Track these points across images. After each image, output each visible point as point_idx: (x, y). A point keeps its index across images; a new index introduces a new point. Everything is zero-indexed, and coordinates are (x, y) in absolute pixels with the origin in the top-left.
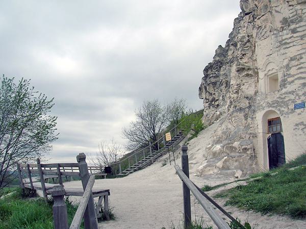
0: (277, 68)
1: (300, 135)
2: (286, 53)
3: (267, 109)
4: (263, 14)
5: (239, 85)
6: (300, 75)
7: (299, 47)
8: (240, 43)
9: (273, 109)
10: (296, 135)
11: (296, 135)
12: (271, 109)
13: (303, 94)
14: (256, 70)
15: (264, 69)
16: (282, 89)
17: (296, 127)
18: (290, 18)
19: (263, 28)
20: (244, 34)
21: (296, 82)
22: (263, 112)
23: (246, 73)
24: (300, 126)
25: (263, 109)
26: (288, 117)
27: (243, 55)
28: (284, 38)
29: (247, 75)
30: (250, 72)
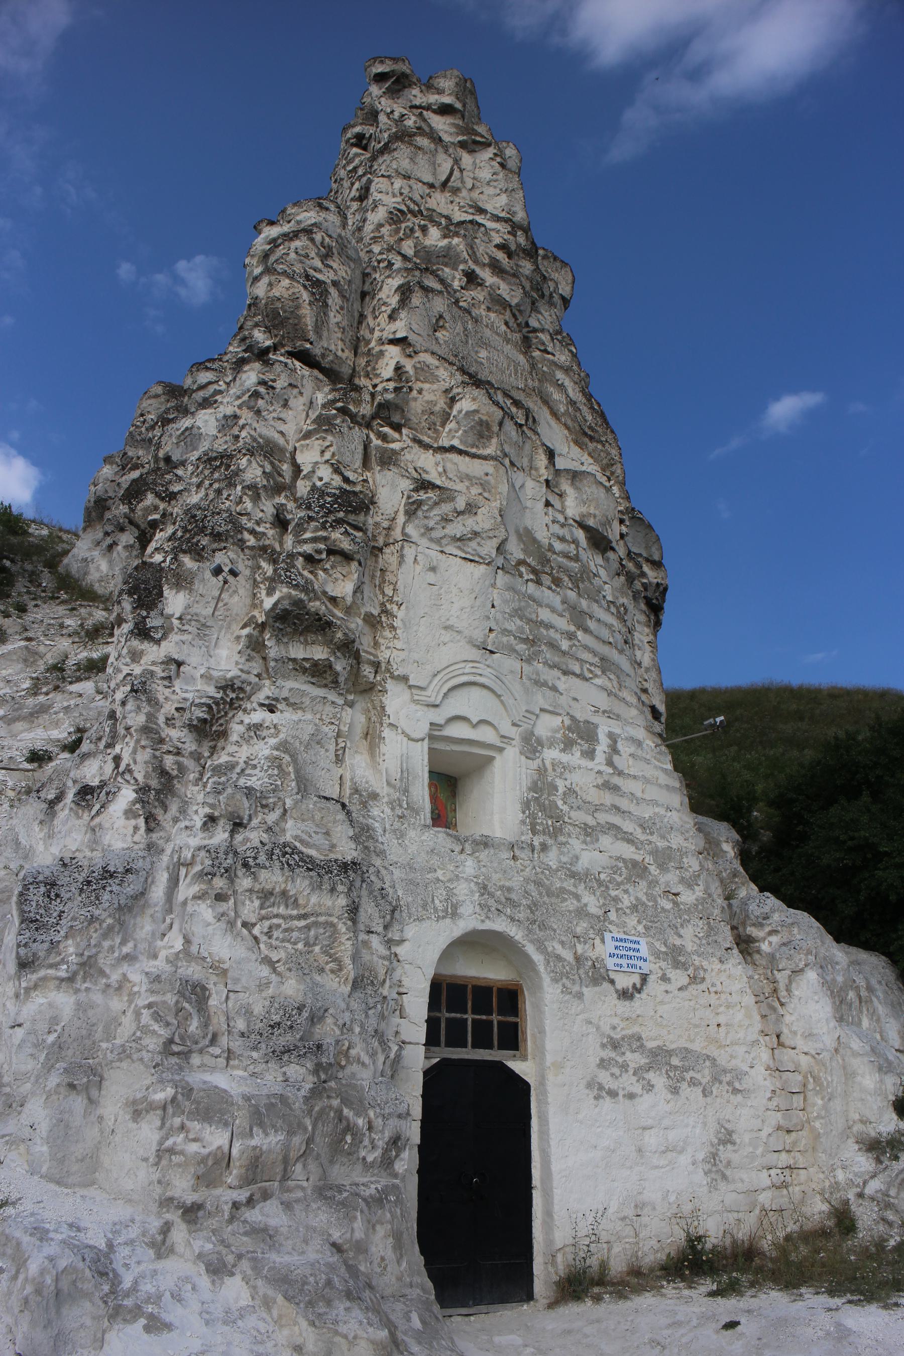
0: (506, 728)
1: (631, 1096)
2: (554, 689)
3: (470, 920)
4: (456, 443)
5: (232, 695)
6: (616, 820)
7: (603, 701)
8: (268, 468)
9: (516, 933)
10: (613, 1094)
11: (613, 1094)
12: (499, 925)
13: (634, 908)
14: (367, 671)
15: (433, 694)
16: (544, 847)
17: (613, 1055)
18: (551, 548)
19: (461, 504)
20: (281, 441)
21: (606, 841)
22: (450, 931)
23: (319, 653)
24: (629, 1056)
25: (453, 912)
26: (580, 996)
27: (331, 552)
28: (545, 615)
29: (318, 672)
30: (340, 666)
